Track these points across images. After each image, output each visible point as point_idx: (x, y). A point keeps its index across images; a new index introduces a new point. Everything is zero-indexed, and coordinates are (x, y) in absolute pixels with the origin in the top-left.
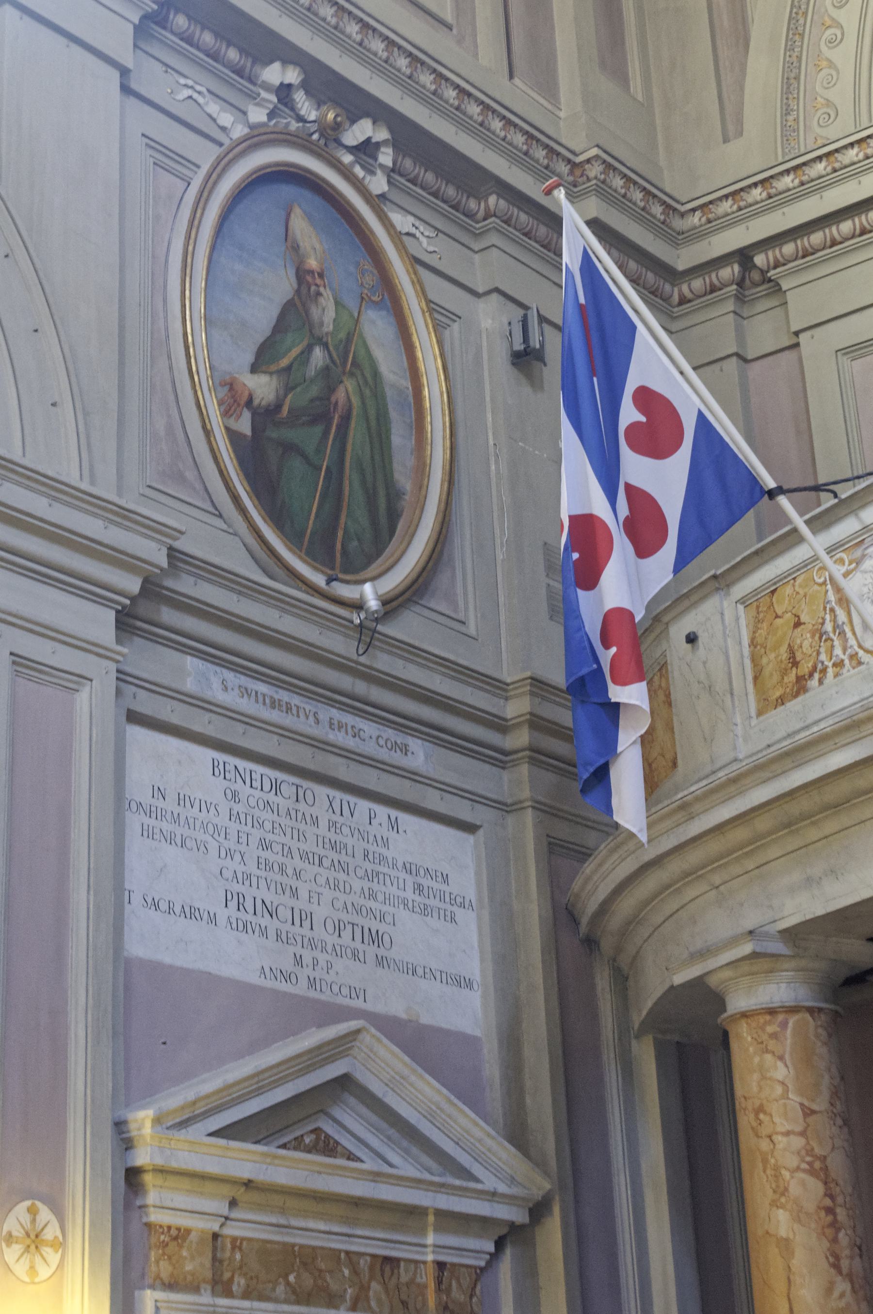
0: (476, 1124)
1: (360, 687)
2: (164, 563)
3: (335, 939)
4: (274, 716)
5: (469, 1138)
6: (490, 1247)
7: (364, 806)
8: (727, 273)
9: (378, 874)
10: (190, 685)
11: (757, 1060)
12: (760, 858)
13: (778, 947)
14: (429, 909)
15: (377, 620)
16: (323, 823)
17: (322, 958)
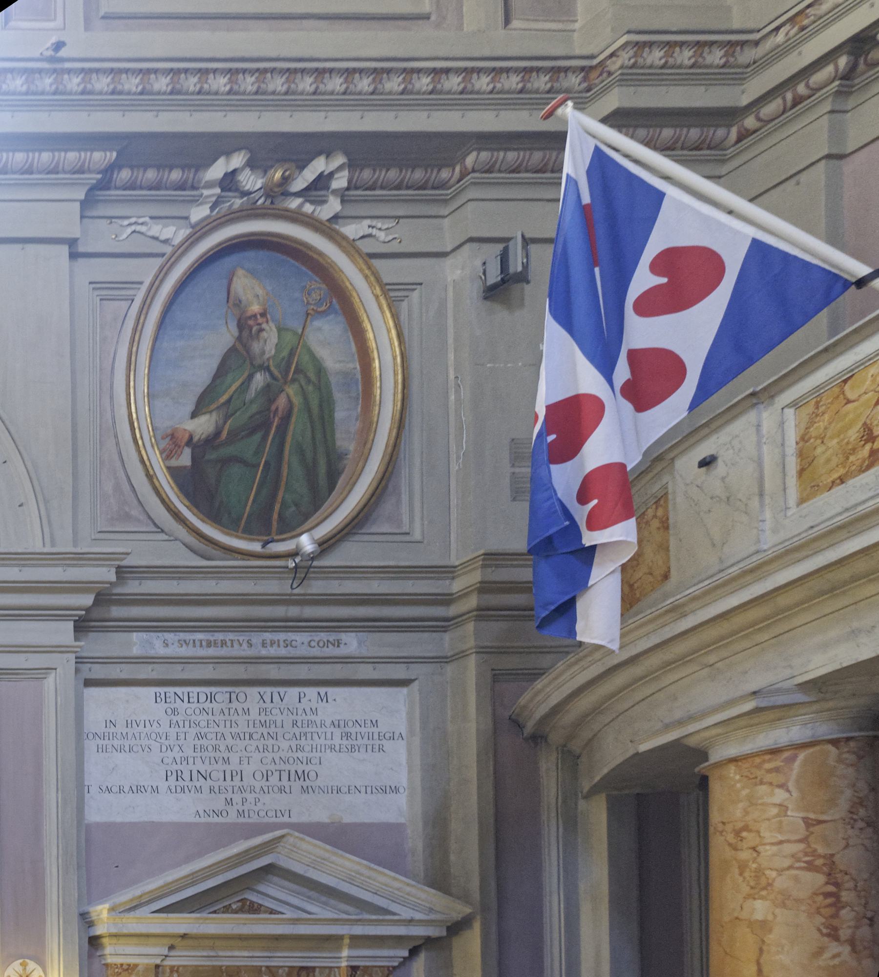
0: (395, 879)
1: (294, 611)
2: (113, 577)
4: (211, 652)
5: (387, 888)
6: (406, 953)
7: (293, 692)
10: (136, 651)
15: (313, 559)
16: (254, 712)
17: (250, 797)
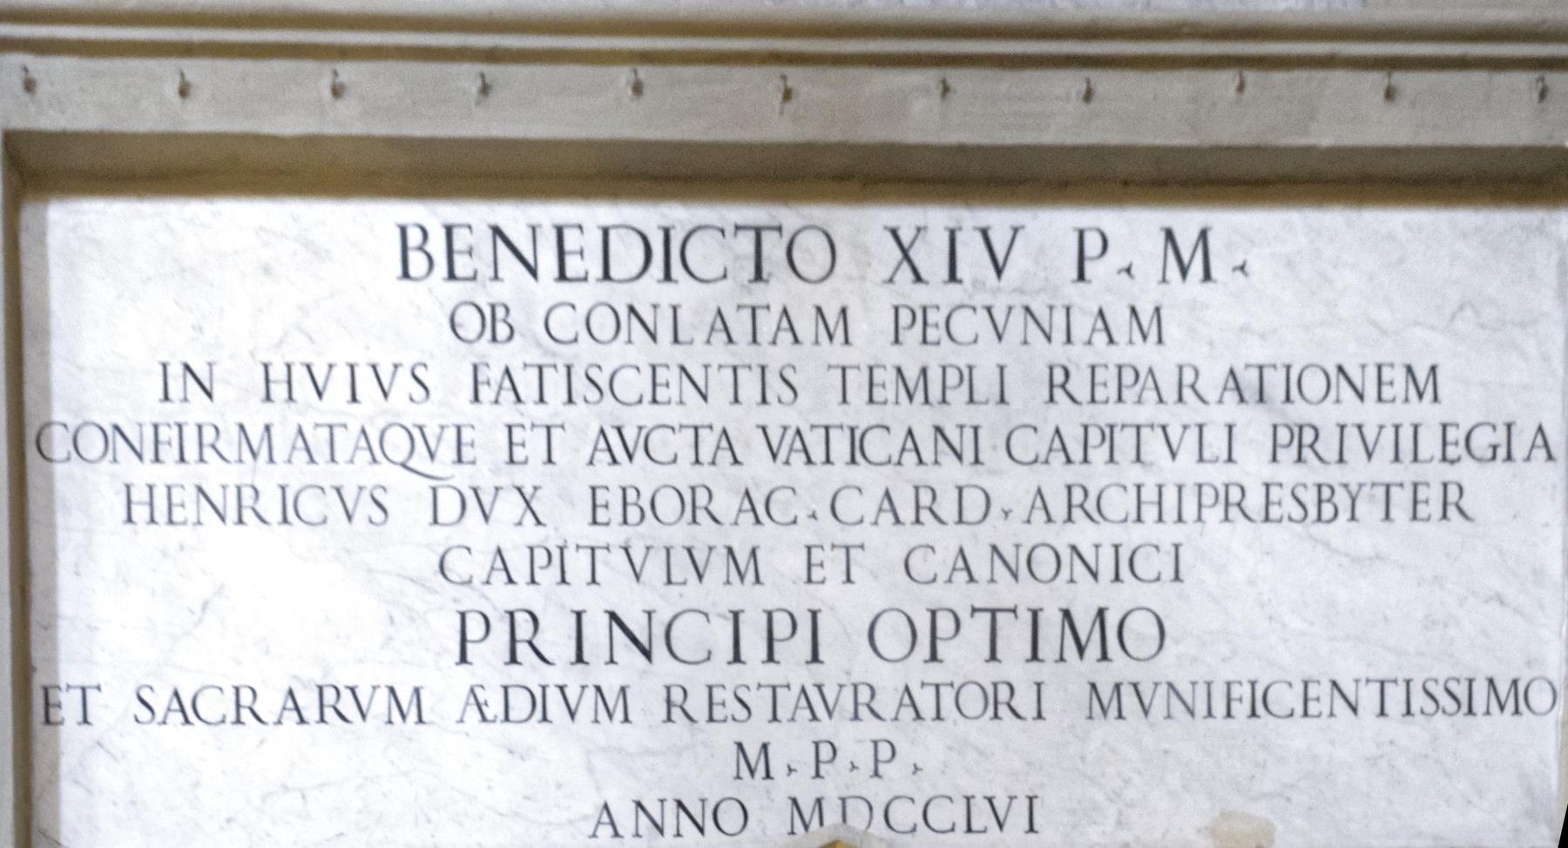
3: (917, 670)
9: (1109, 434)
14: (1342, 499)
16: (870, 326)
17: (853, 738)
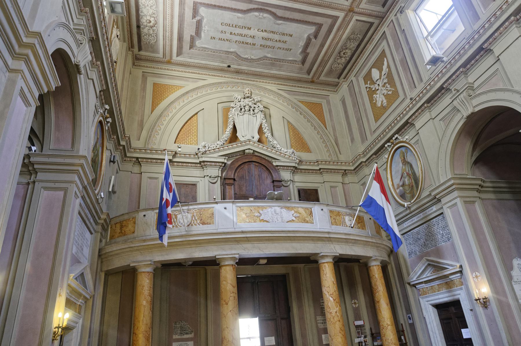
8: (134, 159)
11: (144, 279)
12: (152, 250)
13: (153, 263)
